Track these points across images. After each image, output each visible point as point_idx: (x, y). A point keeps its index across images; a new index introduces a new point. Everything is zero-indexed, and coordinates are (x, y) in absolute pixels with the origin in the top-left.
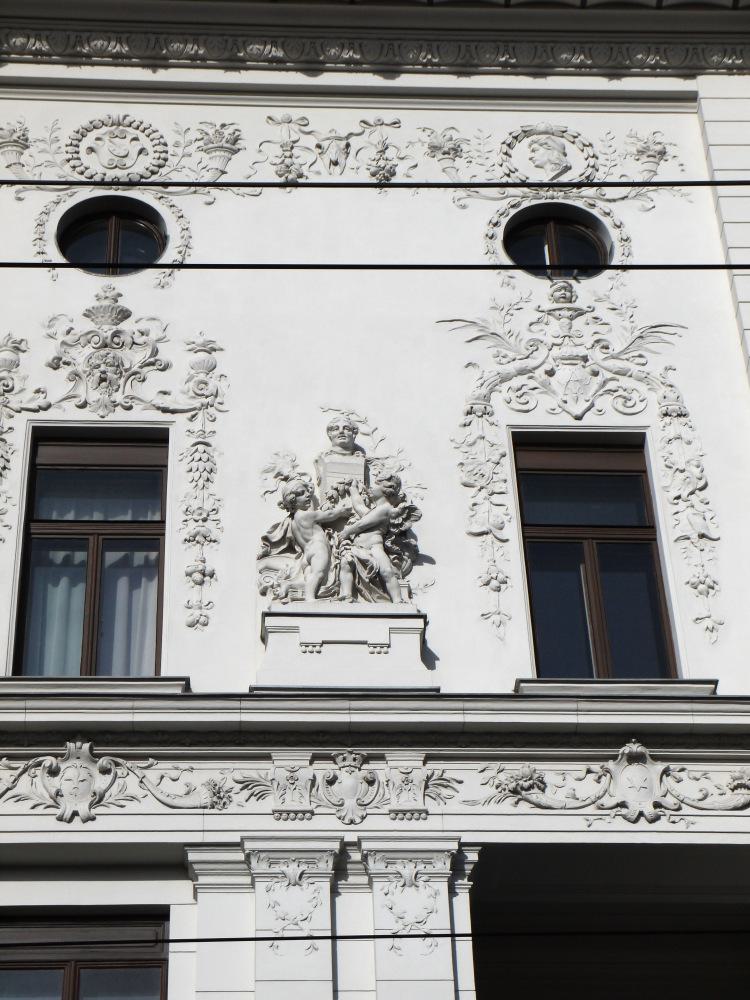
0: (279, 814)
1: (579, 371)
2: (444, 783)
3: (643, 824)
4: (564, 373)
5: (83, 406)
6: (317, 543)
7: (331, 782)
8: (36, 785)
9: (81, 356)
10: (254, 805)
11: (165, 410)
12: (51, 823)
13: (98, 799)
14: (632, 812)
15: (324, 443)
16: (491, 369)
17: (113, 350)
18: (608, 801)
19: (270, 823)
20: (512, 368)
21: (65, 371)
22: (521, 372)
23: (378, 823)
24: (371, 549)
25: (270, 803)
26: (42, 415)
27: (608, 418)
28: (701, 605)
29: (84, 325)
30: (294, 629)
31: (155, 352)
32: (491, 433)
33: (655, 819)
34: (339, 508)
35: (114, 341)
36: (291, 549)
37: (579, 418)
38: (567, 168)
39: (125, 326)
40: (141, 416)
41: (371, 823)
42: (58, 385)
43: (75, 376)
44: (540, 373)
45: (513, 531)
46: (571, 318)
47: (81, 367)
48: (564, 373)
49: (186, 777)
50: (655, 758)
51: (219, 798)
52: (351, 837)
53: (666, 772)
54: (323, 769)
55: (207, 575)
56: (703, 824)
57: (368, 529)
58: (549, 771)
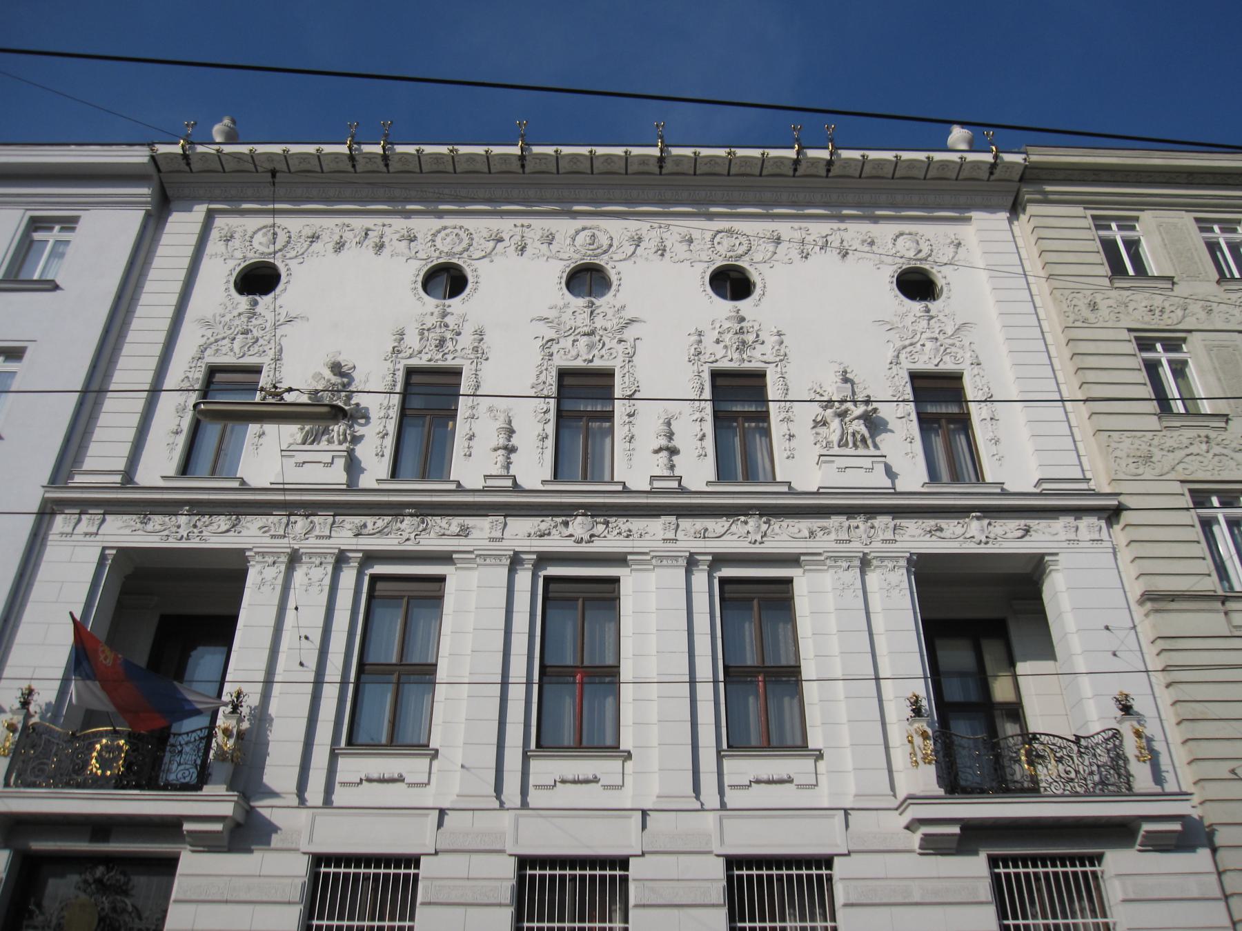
2: (901, 528)
4: (929, 345)
5: (731, 360)
6: (835, 424)
7: (857, 527)
8: (738, 528)
10: (826, 538)
12: (746, 544)
13: (765, 535)
16: (899, 344)
18: (968, 535)
19: (833, 545)
20: (907, 342)
21: (722, 345)
22: (911, 344)
23: (877, 545)
25: (833, 536)
27: (948, 365)
28: (994, 449)
29: (726, 325)
30: (833, 462)
31: (758, 336)
32: (900, 372)
33: (987, 543)
34: (843, 407)
36: (824, 424)
38: (920, 251)
39: (743, 324)
40: (755, 365)
42: (719, 351)
43: (726, 347)
44: (918, 345)
45: (914, 416)
47: (728, 344)
49: (797, 525)
52: (866, 551)
53: (990, 524)
54: (853, 523)
55: (791, 436)
56: (1005, 545)
57: (858, 418)
58: (943, 523)
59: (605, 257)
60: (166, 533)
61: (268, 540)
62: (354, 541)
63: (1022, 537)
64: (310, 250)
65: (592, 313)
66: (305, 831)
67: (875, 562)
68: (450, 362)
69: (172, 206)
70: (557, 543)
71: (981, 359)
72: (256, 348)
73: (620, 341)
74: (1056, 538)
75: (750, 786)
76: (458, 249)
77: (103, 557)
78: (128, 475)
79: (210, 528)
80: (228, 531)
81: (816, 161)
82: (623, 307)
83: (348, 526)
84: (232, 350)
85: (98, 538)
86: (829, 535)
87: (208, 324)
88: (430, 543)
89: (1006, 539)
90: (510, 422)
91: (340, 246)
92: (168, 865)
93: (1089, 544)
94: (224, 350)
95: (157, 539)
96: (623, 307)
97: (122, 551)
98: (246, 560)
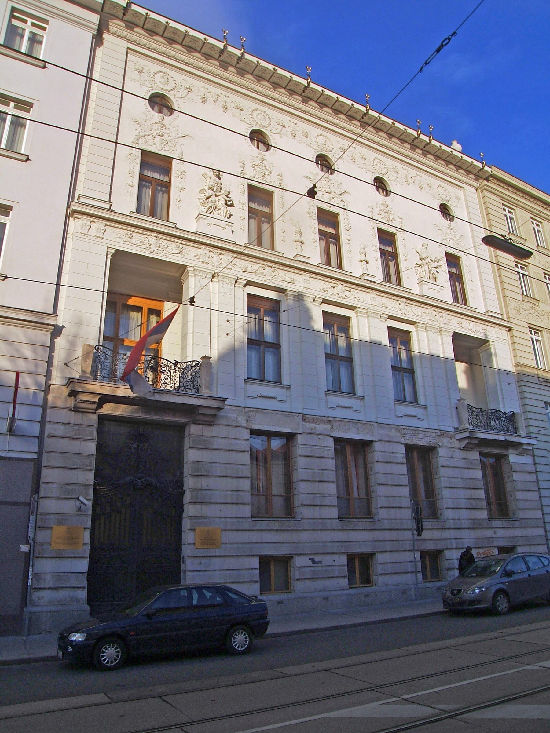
60: (143, 247)
61: (200, 264)
64: (189, 96)
72: (167, 148)
76: (265, 124)
79: (167, 250)
83: (239, 266)
84: (155, 144)
85: (104, 241)
91: (204, 100)
94: (151, 142)
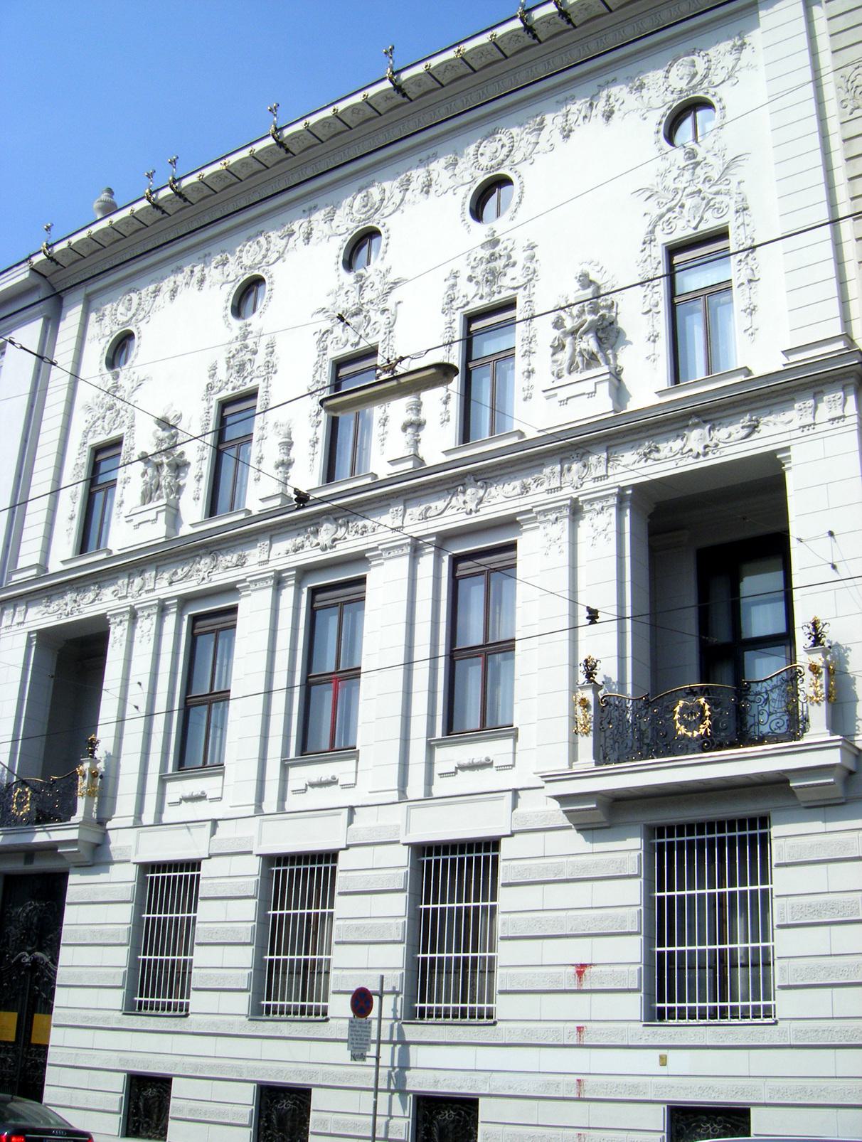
0: (549, 491)
1: (697, 199)
3: (701, 458)
4: (689, 203)
5: (481, 298)
8: (457, 501)
9: (479, 272)
11: (514, 288)
12: (464, 516)
13: (481, 501)
14: (694, 453)
15: (577, 286)
16: (657, 212)
17: (493, 261)
18: (685, 450)
19: (545, 496)
20: (664, 210)
22: (669, 210)
23: (589, 485)
24: (589, 343)
26: (467, 308)
30: (555, 395)
31: (509, 257)
33: (705, 454)
35: (493, 258)
37: (695, 228)
38: (695, 74)
41: (586, 486)
42: (471, 289)
43: (477, 283)
44: (677, 209)
46: (694, 169)
48: (689, 203)
49: (513, 484)
50: (705, 422)
51: (525, 489)
56: (728, 451)
59: (377, 216)
61: (118, 602)
62: (170, 589)
63: (748, 436)
65: (361, 287)
66: (133, 845)
67: (586, 507)
68: (249, 385)
69: (65, 303)
70: (311, 555)
71: (750, 203)
73: (384, 311)
74: (791, 427)
75: (456, 773)
77: (29, 640)
78: (43, 566)
80: (94, 601)
81: (547, 19)
82: (388, 271)
86: (546, 488)
87: (90, 409)
88: (220, 578)
89: (730, 444)
90: (289, 435)
92: (62, 878)
93: (828, 425)
95: (55, 618)
96: (388, 271)
97: (40, 632)
98: (107, 623)
